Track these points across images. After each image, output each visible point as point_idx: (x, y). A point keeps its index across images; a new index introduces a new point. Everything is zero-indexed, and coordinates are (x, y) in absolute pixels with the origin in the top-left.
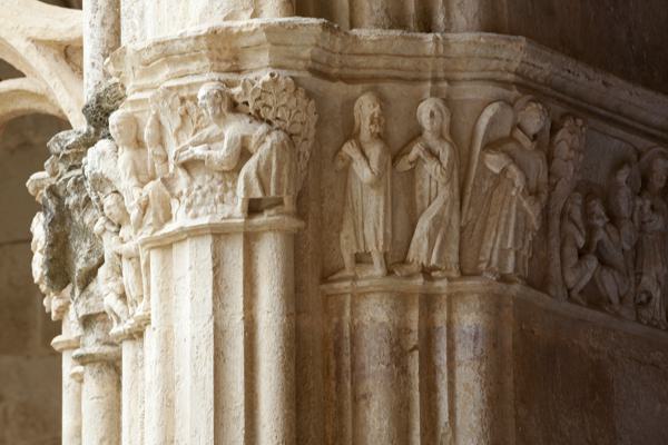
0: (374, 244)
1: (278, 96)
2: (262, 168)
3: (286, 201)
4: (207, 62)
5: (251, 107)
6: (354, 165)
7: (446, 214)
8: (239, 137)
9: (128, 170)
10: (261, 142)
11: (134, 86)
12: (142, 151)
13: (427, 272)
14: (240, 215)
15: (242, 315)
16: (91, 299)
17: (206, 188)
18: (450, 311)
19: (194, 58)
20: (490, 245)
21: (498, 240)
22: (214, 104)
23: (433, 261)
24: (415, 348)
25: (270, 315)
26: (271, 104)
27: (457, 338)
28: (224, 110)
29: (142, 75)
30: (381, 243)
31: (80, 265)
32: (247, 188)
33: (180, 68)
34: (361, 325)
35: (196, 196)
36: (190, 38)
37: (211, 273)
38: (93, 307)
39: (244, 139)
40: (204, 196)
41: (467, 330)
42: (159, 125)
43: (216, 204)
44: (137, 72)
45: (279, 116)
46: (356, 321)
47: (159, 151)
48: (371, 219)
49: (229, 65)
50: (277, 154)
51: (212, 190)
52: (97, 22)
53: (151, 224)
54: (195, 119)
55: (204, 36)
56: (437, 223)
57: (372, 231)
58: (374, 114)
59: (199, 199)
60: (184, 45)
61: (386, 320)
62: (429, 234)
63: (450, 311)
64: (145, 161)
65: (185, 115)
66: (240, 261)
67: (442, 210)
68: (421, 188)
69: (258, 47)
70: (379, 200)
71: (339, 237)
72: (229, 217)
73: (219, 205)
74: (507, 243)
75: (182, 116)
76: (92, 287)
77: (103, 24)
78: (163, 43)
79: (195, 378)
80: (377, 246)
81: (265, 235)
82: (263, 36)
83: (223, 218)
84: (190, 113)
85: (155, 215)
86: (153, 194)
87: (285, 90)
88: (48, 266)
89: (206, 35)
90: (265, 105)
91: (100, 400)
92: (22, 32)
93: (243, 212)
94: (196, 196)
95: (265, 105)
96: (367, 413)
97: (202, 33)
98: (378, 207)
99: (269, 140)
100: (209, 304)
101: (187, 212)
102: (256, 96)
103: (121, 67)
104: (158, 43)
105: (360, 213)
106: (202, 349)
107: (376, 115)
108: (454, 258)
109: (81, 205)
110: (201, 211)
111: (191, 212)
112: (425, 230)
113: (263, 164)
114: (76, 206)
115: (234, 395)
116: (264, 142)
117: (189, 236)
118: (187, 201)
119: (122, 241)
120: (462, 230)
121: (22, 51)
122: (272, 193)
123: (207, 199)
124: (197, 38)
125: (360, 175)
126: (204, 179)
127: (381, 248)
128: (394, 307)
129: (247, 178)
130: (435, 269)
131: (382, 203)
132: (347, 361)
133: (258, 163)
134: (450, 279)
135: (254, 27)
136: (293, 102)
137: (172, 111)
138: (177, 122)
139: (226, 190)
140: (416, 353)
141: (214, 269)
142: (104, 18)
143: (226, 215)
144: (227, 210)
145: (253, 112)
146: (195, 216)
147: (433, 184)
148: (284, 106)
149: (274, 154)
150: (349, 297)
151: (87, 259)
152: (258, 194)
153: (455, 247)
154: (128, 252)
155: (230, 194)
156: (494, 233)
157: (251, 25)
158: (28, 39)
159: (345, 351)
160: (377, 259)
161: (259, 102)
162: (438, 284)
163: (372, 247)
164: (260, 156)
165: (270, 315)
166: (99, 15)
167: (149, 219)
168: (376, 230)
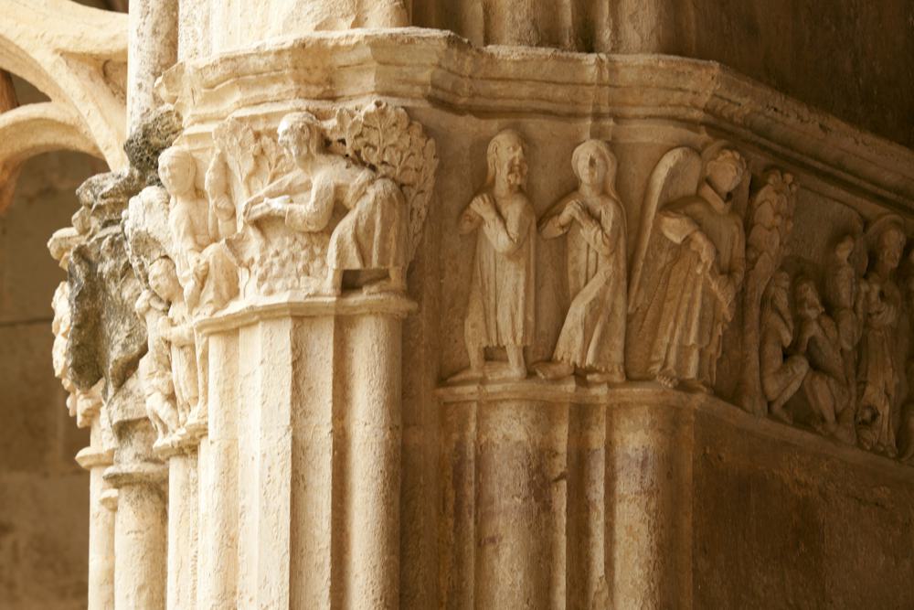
0: (509, 335)
1: (385, 132)
2: (361, 230)
3: (393, 274)
4: (291, 85)
5: (348, 146)
6: (486, 228)
7: (608, 296)
8: (332, 186)
9: (183, 227)
10: (362, 193)
11: (193, 116)
12: (201, 203)
13: (580, 375)
15: (330, 428)
16: (129, 400)
17: (285, 254)
18: (611, 428)
19: (274, 80)
20: (666, 339)
21: (678, 333)
22: (299, 142)
23: (590, 360)
24: (562, 476)
25: (368, 428)
26: (375, 143)
27: (618, 464)
28: (313, 149)
30: (520, 334)
31: (115, 354)
32: (341, 256)
33: (256, 93)
34: (490, 444)
35: (272, 264)
36: (268, 53)
37: (290, 368)
38: (132, 411)
39: (339, 190)
40: (283, 265)
41: (633, 455)
42: (225, 169)
43: (298, 277)
44: (198, 98)
45: (386, 159)
46: (484, 439)
47: (223, 203)
48: (508, 301)
49: (321, 90)
50: (382, 212)
51: (294, 258)
52: (147, 30)
53: (211, 302)
54: (273, 162)
55: (289, 50)
56: (596, 308)
57: (508, 317)
58: (514, 158)
59: (276, 269)
60: (262, 62)
61: (524, 437)
62: (584, 324)
63: (611, 428)
64: (205, 217)
65: (260, 155)
66: (330, 355)
67: (603, 292)
68: (575, 261)
69: (360, 66)
70: (518, 275)
71: (463, 324)
72: (316, 294)
73: (303, 278)
74: (688, 338)
75: (255, 157)
76: (131, 384)
77: (155, 33)
78: (234, 59)
79: (265, 510)
80: (515, 339)
81: (364, 320)
82: (369, 50)
83: (308, 296)
84: (267, 153)
85: (217, 289)
86: (215, 261)
87: (395, 125)
88: (73, 354)
89: (292, 49)
90: (367, 145)
91: (139, 536)
92: (49, 42)
93: (335, 287)
94: (272, 264)
95: (367, 145)
96: (496, 561)
97: (285, 47)
98: (516, 285)
99: (372, 192)
100: (286, 411)
101: (259, 286)
102: (357, 131)
103: (177, 91)
104: (227, 59)
105: (492, 292)
106: (276, 471)
107: (517, 162)
108: (617, 356)
109: (119, 274)
110: (278, 285)
111: (265, 287)
112: (579, 319)
113: (362, 224)
114: (113, 274)
115: (317, 533)
116: (365, 193)
117: (262, 319)
118: (260, 271)
119: (172, 323)
120: (629, 319)
121: (47, 68)
122: (375, 263)
123: (287, 270)
124: (279, 53)
125: (493, 241)
126: (283, 243)
127: (519, 341)
128: (536, 421)
129: (341, 242)
130: (591, 370)
131: (522, 280)
132: (470, 492)
133: (357, 222)
134: (611, 385)
135: (354, 41)
136: (406, 141)
137: (243, 148)
138: (249, 165)
139: (312, 257)
140: (564, 483)
141: (294, 364)
142: (157, 24)
143: (311, 291)
144: (313, 285)
145: (351, 154)
146: (270, 292)
147: (592, 256)
148: (393, 146)
149: (379, 210)
150: (474, 406)
151: (125, 346)
152: (355, 263)
153: (619, 342)
154: (180, 338)
155: (317, 264)
156: (671, 324)
157: (352, 37)
158: (56, 51)
159: (468, 478)
160: (513, 355)
161: (359, 141)
162: (595, 391)
163: (507, 340)
164: (360, 213)
165: (368, 428)
166: (150, 20)
167: (209, 294)
168: (513, 316)
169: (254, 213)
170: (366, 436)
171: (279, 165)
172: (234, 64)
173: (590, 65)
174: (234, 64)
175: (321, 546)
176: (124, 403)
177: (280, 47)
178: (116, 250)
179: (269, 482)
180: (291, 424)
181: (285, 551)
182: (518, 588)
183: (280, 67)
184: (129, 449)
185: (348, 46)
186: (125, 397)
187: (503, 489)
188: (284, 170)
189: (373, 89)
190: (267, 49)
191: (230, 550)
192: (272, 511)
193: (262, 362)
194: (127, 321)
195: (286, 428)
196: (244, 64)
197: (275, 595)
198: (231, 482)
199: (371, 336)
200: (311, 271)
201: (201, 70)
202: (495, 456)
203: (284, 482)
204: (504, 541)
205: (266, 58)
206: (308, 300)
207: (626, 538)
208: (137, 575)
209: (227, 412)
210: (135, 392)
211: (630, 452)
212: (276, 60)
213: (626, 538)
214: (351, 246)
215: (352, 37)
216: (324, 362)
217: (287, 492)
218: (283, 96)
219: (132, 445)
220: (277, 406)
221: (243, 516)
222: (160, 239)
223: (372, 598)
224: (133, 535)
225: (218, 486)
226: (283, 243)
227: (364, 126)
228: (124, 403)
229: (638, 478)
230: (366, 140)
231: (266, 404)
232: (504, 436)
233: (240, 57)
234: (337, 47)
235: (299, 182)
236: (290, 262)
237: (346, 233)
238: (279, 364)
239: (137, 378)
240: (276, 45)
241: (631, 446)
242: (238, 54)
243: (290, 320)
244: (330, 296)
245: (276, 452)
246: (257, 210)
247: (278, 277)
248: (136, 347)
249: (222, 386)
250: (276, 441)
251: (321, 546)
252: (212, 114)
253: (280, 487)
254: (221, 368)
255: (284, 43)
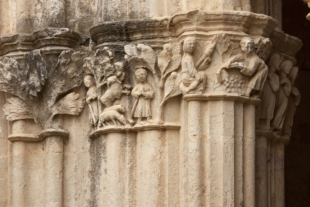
4: (241, 27)
14: (248, 95)
16: (60, 107)
17: (235, 80)
19: (236, 24)
25: (252, 140)
29: (201, 24)
33: (229, 27)
35: (231, 83)
36: (241, 15)
44: (199, 22)
45: (263, 57)
51: (238, 82)
59: (232, 85)
60: (237, 18)
76: (61, 102)
78: (228, 15)
82: (267, 22)
83: (242, 95)
86: (204, 78)
91: (60, 154)
94: (231, 83)
96: (260, 185)
97: (247, 15)
101: (226, 89)
102: (262, 47)
103: (190, 18)
104: (226, 14)
106: (229, 149)
110: (233, 90)
111: (229, 90)
114: (64, 64)
115: (239, 171)
118: (227, 85)
124: (244, 17)
131: (275, 100)
135: (264, 18)
137: (225, 44)
143: (243, 94)
146: (230, 92)
148: (266, 53)
157: (264, 17)
165: (252, 140)
169: (232, 66)
170: (251, 142)
171: (234, 51)
172: (227, 16)
173: (287, 37)
174: (227, 16)
175: (240, 175)
176: (58, 108)
177: (245, 15)
178: (67, 56)
179: (227, 152)
180: (234, 135)
181: (232, 175)
182: (265, 194)
183: (241, 21)
184: (57, 124)
185: (262, 19)
186: (58, 106)
187: (262, 163)
188: (234, 53)
189: (262, 34)
190: (241, 14)
191: (202, 171)
192: (228, 162)
193: (223, 114)
194: (64, 81)
195: (232, 136)
196: (231, 17)
197: (229, 188)
198: (202, 149)
199: (253, 111)
200: (241, 87)
201: (207, 14)
202: (259, 153)
203: (232, 153)
204: (262, 179)
205: (239, 17)
206: (241, 97)
207: (279, 182)
208: (59, 167)
209: (201, 127)
210: (62, 105)
211: (279, 156)
212: (242, 18)
213: (279, 182)
214: (259, 83)
215: (264, 17)
216: (240, 117)
217: (233, 156)
218: (238, 30)
219: (58, 122)
220: (229, 128)
221: (212, 161)
222: (148, 62)
223: (253, 194)
224: (58, 153)
225: (198, 150)
226: (235, 77)
227: (264, 46)
228: (58, 108)
229: (281, 165)
230: (262, 50)
231: (225, 127)
232: (262, 147)
233: (230, 15)
234: (258, 19)
235: (241, 59)
236: (236, 83)
237: (259, 78)
238: (230, 115)
239: (64, 100)
240: (244, 14)
241: (280, 155)
242: (230, 14)
243: (234, 102)
244: (247, 97)
245: (229, 143)
246: (233, 65)
247: (232, 87)
248: (67, 90)
249: (199, 118)
250: (229, 139)
251: (240, 175)
252: (204, 29)
253: (230, 155)
254: (199, 112)
255: (246, 14)
